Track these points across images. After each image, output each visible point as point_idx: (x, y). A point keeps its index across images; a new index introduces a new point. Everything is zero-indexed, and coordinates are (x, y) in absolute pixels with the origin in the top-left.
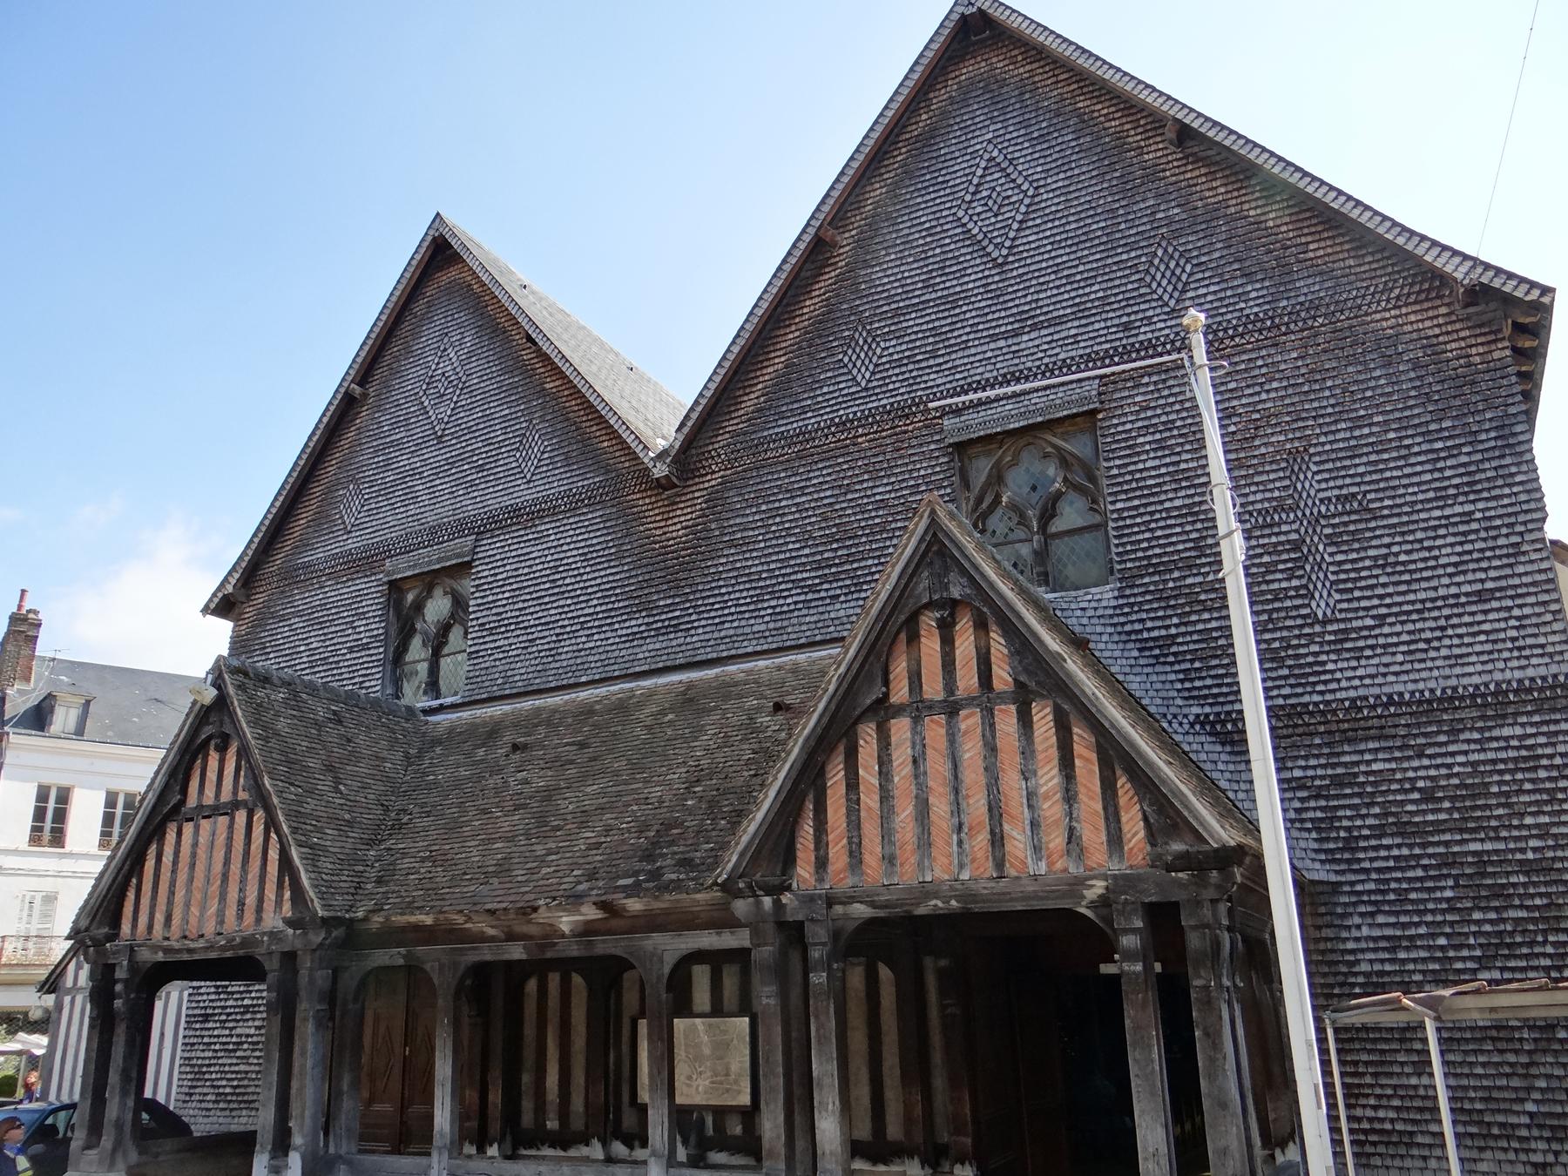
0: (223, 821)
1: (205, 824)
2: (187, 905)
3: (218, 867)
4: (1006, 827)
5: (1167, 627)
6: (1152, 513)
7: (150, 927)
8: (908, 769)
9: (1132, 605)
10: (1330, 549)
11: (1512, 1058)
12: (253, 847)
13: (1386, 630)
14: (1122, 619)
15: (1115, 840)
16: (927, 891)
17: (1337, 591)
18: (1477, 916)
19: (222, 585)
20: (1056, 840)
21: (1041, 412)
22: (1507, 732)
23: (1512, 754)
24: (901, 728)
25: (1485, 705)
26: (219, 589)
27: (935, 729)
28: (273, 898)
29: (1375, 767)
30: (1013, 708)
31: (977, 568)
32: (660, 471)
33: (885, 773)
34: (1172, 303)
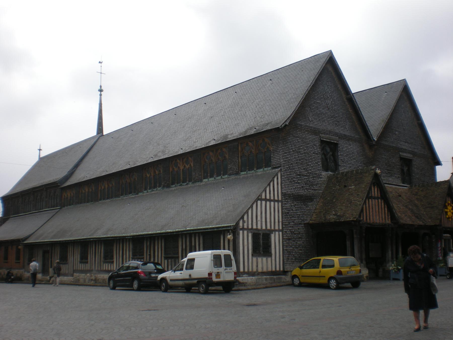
3: (377, 210)
32: (374, 143)
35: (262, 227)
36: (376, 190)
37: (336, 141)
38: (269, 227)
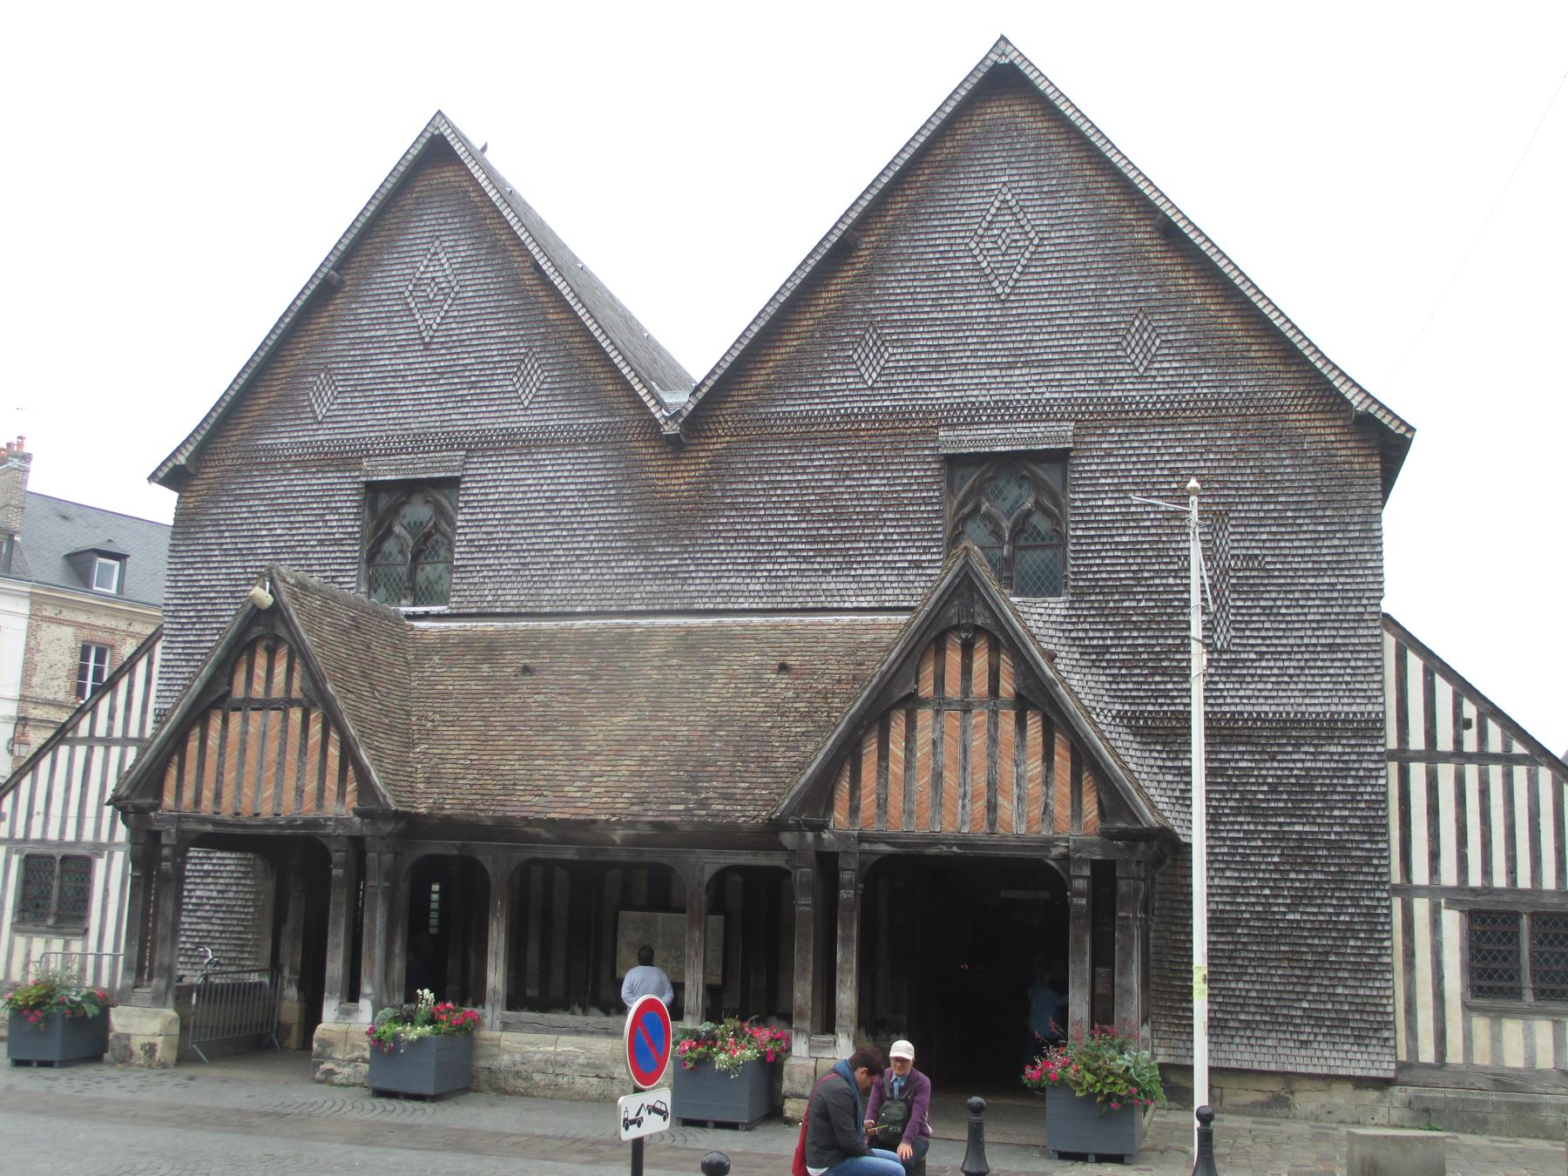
0: (275, 716)
1: (256, 717)
2: (239, 786)
4: (1000, 798)
5: (1105, 638)
6: (1103, 544)
7: (197, 800)
8: (929, 748)
9: (1079, 616)
10: (1234, 596)
11: (1298, 972)
12: (311, 742)
13: (1264, 664)
14: (1070, 627)
15: (1077, 813)
16: (934, 840)
17: (1235, 629)
18: (1292, 876)
19: (173, 455)
20: (1036, 812)
21: (1024, 441)
22: (1333, 749)
23: (1333, 765)
24: (925, 717)
25: (1322, 728)
26: (169, 459)
27: (952, 721)
28: (335, 788)
29: (1241, 764)
30: (1012, 713)
31: (997, 605)
32: (670, 429)
33: (910, 749)
34: (1141, 369)
35: (62, 831)
36: (280, 668)
37: (446, 469)
38: (88, 836)
